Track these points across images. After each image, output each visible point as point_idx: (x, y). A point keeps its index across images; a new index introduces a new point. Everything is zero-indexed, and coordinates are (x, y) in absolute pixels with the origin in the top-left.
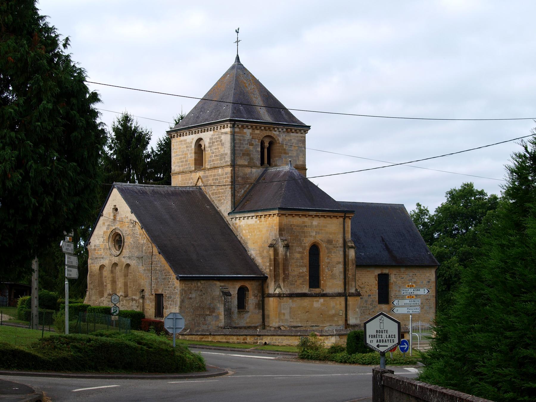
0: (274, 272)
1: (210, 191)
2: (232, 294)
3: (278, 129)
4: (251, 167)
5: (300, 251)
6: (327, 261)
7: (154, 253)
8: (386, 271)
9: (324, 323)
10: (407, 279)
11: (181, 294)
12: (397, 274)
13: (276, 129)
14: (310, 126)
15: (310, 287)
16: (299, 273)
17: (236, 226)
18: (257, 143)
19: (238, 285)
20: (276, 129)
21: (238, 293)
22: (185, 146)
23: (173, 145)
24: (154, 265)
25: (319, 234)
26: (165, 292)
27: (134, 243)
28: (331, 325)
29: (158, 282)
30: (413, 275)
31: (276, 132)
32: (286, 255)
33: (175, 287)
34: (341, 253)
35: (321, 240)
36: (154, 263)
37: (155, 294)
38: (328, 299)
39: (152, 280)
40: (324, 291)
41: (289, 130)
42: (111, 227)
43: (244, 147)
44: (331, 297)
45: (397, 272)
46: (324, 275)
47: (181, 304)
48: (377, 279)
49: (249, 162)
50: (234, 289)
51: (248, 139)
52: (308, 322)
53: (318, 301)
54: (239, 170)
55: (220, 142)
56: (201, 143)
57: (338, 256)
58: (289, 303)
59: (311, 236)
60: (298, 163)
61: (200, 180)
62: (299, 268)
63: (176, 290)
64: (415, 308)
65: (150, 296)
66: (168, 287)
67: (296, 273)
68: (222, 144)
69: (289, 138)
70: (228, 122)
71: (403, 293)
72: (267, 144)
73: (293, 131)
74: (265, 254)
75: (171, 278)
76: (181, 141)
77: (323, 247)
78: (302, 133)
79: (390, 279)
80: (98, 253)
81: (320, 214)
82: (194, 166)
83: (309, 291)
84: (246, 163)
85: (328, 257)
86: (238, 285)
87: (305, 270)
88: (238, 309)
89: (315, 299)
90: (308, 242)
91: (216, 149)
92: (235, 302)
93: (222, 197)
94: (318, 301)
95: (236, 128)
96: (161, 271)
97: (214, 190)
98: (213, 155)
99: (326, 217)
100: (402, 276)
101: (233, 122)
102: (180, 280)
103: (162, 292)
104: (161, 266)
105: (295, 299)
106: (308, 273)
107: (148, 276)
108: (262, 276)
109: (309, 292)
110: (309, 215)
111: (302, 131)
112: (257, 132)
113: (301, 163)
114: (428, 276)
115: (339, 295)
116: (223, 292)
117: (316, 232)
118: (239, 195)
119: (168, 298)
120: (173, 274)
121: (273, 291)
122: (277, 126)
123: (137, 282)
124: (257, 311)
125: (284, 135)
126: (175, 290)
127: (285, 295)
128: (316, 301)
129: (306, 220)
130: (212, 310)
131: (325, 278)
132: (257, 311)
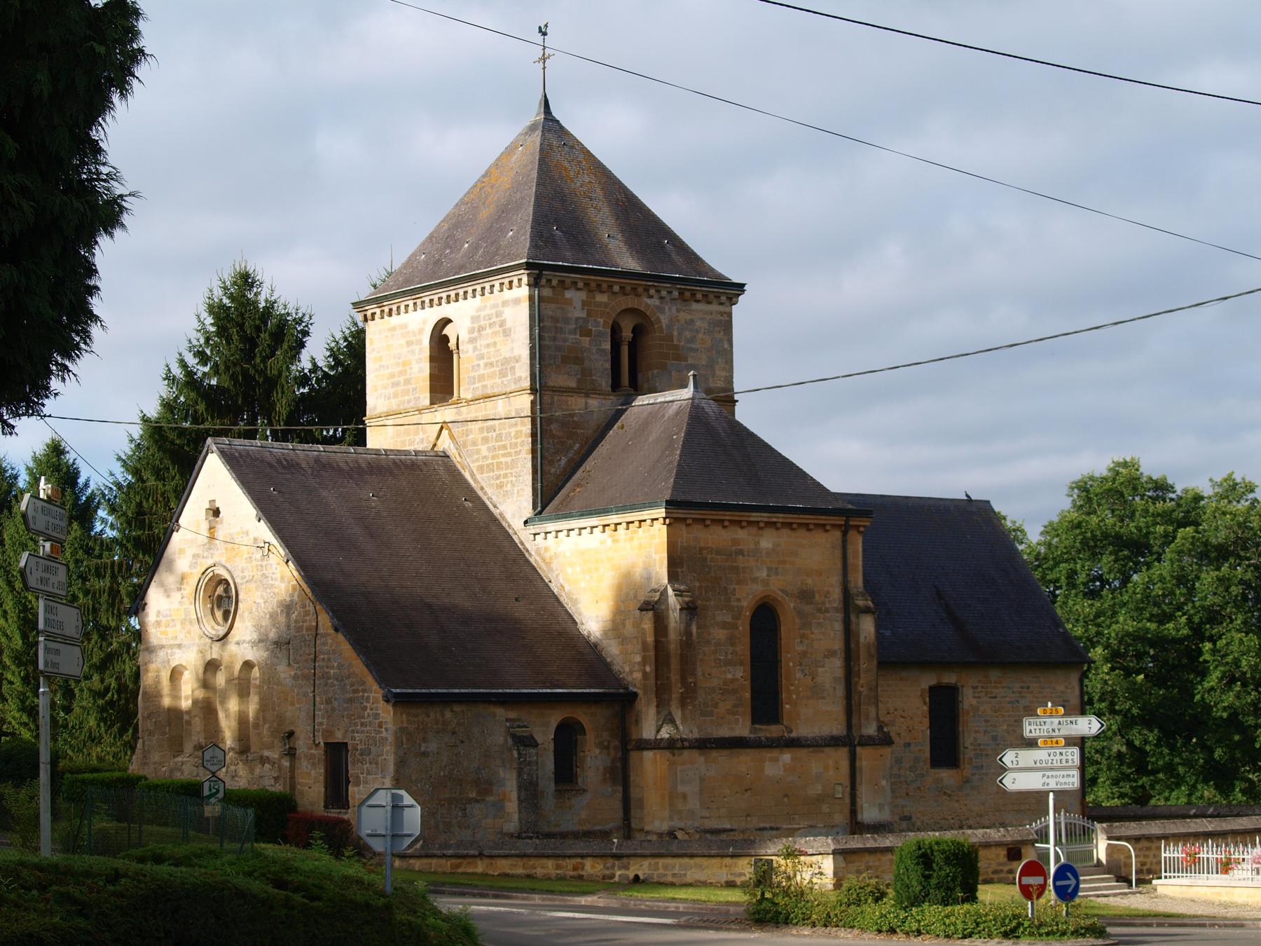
0: (657, 678)
1: (473, 462)
2: (539, 742)
3: (658, 291)
4: (587, 395)
5: (726, 622)
6: (800, 648)
7: (321, 631)
8: (949, 678)
9: (794, 819)
10: (1007, 699)
11: (398, 743)
12: (980, 685)
13: (652, 292)
14: (744, 285)
15: (753, 722)
16: (725, 683)
17: (547, 555)
18: (601, 326)
19: (555, 718)
20: (652, 292)
21: (555, 739)
22: (403, 341)
24: (321, 663)
25: (777, 574)
26: (353, 738)
27: (265, 602)
28: (811, 826)
29: (333, 710)
30: (1022, 688)
31: (653, 300)
32: (688, 633)
33: (380, 726)
34: (838, 626)
35: (782, 591)
36: (322, 657)
37: (325, 743)
38: (802, 753)
39: (317, 703)
40: (791, 731)
41: (687, 294)
42: (203, 561)
43: (565, 340)
44: (811, 749)
45: (979, 681)
46: (792, 688)
47: (397, 771)
48: (928, 700)
49: (579, 381)
50: (544, 729)
51: (577, 319)
52: (749, 819)
53: (776, 760)
54: (552, 403)
55: (501, 326)
56: (448, 331)
57: (828, 636)
58: (697, 765)
59: (755, 580)
60: (712, 385)
61: (445, 432)
62: (724, 669)
64: (1065, 773)
66: (362, 724)
67: (715, 682)
68: (507, 333)
69: (689, 317)
70: (522, 271)
71: (1031, 731)
72: (627, 334)
73: (699, 296)
74: (629, 629)
75: (368, 698)
76: (394, 329)
77: (789, 609)
78: (721, 304)
79: (960, 699)
80: (166, 633)
81: (779, 518)
82: (428, 395)
83: (751, 732)
84: (573, 384)
85: (803, 636)
86: (555, 718)
87: (740, 674)
88: (556, 782)
89: (769, 755)
90: (746, 597)
91: (488, 346)
92: (549, 764)
93: (506, 476)
94: (776, 760)
95: (543, 286)
96: (342, 680)
97: (485, 457)
98: (482, 363)
99: (795, 526)
100: (994, 690)
101: (537, 272)
102: (394, 705)
103: (344, 738)
104: (340, 666)
105: (714, 754)
106: (748, 683)
107: (305, 695)
108: (622, 691)
109: (752, 736)
110: (750, 523)
111: (723, 298)
112: (602, 298)
113: (720, 384)
114: (1062, 692)
115: (834, 742)
116: (513, 736)
117: (769, 569)
118: (553, 470)
119: (361, 754)
120: (375, 687)
121: (653, 732)
122: (656, 284)
124: (610, 789)
125: (674, 309)
126: (381, 732)
127: (686, 744)
128: (771, 760)
129: (741, 534)
130: (485, 786)
131: (794, 697)
132: (610, 789)
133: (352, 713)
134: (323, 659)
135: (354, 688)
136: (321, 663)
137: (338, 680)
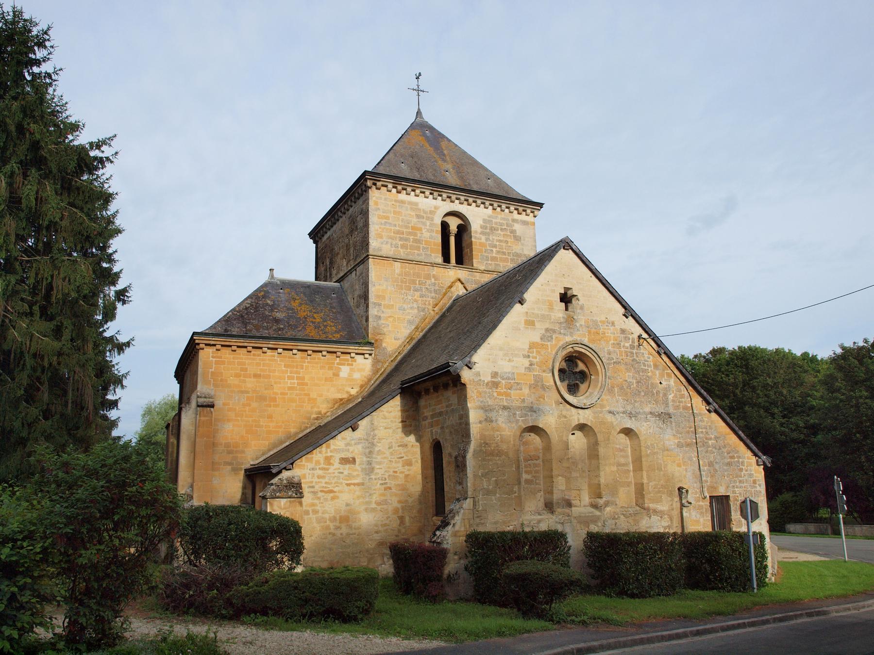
24: (701, 435)
26: (734, 492)
27: (638, 382)
33: (755, 482)
36: (700, 430)
37: (710, 496)
42: (561, 336)
63: (758, 487)
65: (699, 501)
75: (743, 463)
96: (720, 449)
104: (716, 438)
123: (660, 469)
134: (702, 432)
135: (731, 455)
136: (701, 435)
137: (716, 449)
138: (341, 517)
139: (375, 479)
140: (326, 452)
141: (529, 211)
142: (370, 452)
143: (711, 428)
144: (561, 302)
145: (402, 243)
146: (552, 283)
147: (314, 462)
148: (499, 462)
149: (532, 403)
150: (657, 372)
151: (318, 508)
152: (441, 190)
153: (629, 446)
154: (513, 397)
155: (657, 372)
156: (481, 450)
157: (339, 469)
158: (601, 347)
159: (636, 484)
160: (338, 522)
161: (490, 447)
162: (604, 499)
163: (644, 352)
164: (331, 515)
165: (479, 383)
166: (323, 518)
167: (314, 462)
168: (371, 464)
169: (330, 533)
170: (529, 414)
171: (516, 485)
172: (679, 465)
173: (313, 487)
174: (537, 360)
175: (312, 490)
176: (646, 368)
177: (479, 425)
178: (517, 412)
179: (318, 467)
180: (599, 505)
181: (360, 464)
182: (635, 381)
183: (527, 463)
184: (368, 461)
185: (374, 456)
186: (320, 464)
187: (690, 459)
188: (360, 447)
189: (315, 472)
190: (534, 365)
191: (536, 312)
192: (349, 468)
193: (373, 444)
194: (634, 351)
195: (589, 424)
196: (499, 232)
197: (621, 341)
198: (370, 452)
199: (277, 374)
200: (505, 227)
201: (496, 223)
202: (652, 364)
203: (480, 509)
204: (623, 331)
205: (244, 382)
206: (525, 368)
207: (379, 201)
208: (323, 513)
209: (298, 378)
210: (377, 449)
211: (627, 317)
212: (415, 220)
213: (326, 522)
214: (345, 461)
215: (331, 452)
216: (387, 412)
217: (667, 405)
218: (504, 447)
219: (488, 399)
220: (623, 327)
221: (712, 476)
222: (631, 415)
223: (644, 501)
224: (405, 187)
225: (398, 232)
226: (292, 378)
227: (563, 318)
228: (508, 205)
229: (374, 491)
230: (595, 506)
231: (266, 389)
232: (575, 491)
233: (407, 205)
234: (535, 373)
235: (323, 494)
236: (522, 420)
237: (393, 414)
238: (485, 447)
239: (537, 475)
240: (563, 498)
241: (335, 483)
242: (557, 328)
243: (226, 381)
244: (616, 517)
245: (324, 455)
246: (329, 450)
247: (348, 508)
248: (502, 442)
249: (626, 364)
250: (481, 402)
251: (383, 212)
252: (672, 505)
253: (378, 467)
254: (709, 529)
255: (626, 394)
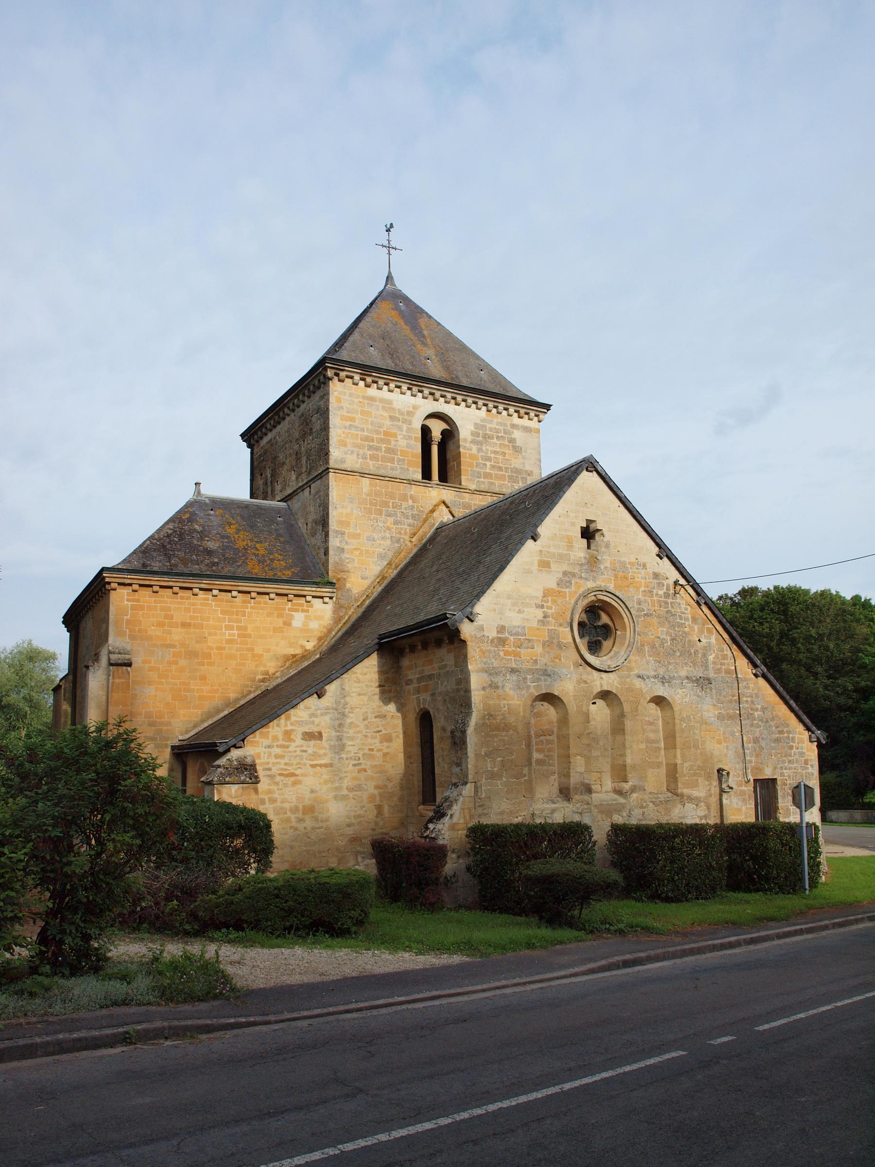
23: (339, 400)
24: (746, 705)
26: (782, 774)
27: (673, 640)
29: (762, 748)
33: (806, 762)
36: (745, 699)
42: (582, 582)
65: (741, 785)
66: (790, 762)
75: (793, 738)
96: (767, 722)
103: (774, 774)
104: (764, 709)
107: (732, 734)
123: (696, 747)
126: (807, 768)
133: (779, 751)
134: (747, 701)
135: (779, 729)
136: (746, 705)
137: (762, 722)
138: (304, 807)
139: (347, 759)
140: (286, 725)
141: (532, 414)
142: (341, 725)
143: (757, 696)
144: (582, 537)
145: (371, 453)
146: (572, 515)
147: (270, 737)
148: (506, 738)
149: (546, 664)
150: (696, 627)
151: (276, 795)
152: (422, 384)
153: (660, 719)
154: (523, 658)
155: (696, 627)
156: (484, 724)
157: (302, 746)
158: (630, 595)
159: (667, 765)
160: (301, 813)
161: (495, 719)
162: (630, 783)
163: (681, 602)
164: (292, 805)
165: (482, 639)
166: (282, 808)
167: (270, 737)
168: (341, 740)
169: (291, 827)
170: (543, 678)
171: (526, 766)
172: (719, 742)
173: (270, 769)
174: (553, 611)
175: (269, 773)
176: (683, 622)
177: (482, 692)
178: (529, 677)
179: (275, 744)
180: (624, 791)
181: (327, 741)
182: (669, 638)
183: (538, 739)
184: (338, 736)
185: (345, 729)
186: (278, 740)
187: (732, 734)
188: (327, 718)
189: (272, 750)
190: (549, 617)
191: (552, 550)
192: (314, 746)
193: (344, 715)
194: (669, 601)
195: (614, 691)
196: (495, 440)
197: (654, 588)
198: (341, 725)
199: (211, 622)
200: (502, 434)
201: (491, 430)
202: (690, 616)
203: (483, 796)
204: (656, 575)
205: (170, 633)
206: (538, 621)
207: (343, 397)
208: (282, 802)
209: (238, 628)
210: (349, 721)
211: (661, 558)
212: (388, 423)
213: (286, 813)
214: (309, 736)
215: (292, 724)
216: (361, 674)
217: (706, 667)
218: (512, 720)
219: (493, 660)
220: (656, 571)
221: (757, 756)
222: (663, 680)
223: (677, 785)
224: (376, 379)
225: (367, 439)
226: (232, 628)
227: (585, 558)
228: (506, 406)
229: (346, 774)
230: (619, 792)
231: (197, 642)
232: (595, 774)
233: (377, 403)
234: (550, 628)
235: (282, 778)
236: (534, 686)
237: (368, 677)
238: (489, 719)
239: (551, 753)
240: (581, 782)
241: (296, 765)
242: (576, 570)
243: (146, 631)
244: (644, 805)
245: (283, 729)
246: (288, 723)
247: (314, 795)
248: (509, 713)
249: (659, 617)
250: (485, 664)
251: (348, 412)
252: (709, 790)
253: (350, 743)
254: (752, 819)
255: (659, 654)
